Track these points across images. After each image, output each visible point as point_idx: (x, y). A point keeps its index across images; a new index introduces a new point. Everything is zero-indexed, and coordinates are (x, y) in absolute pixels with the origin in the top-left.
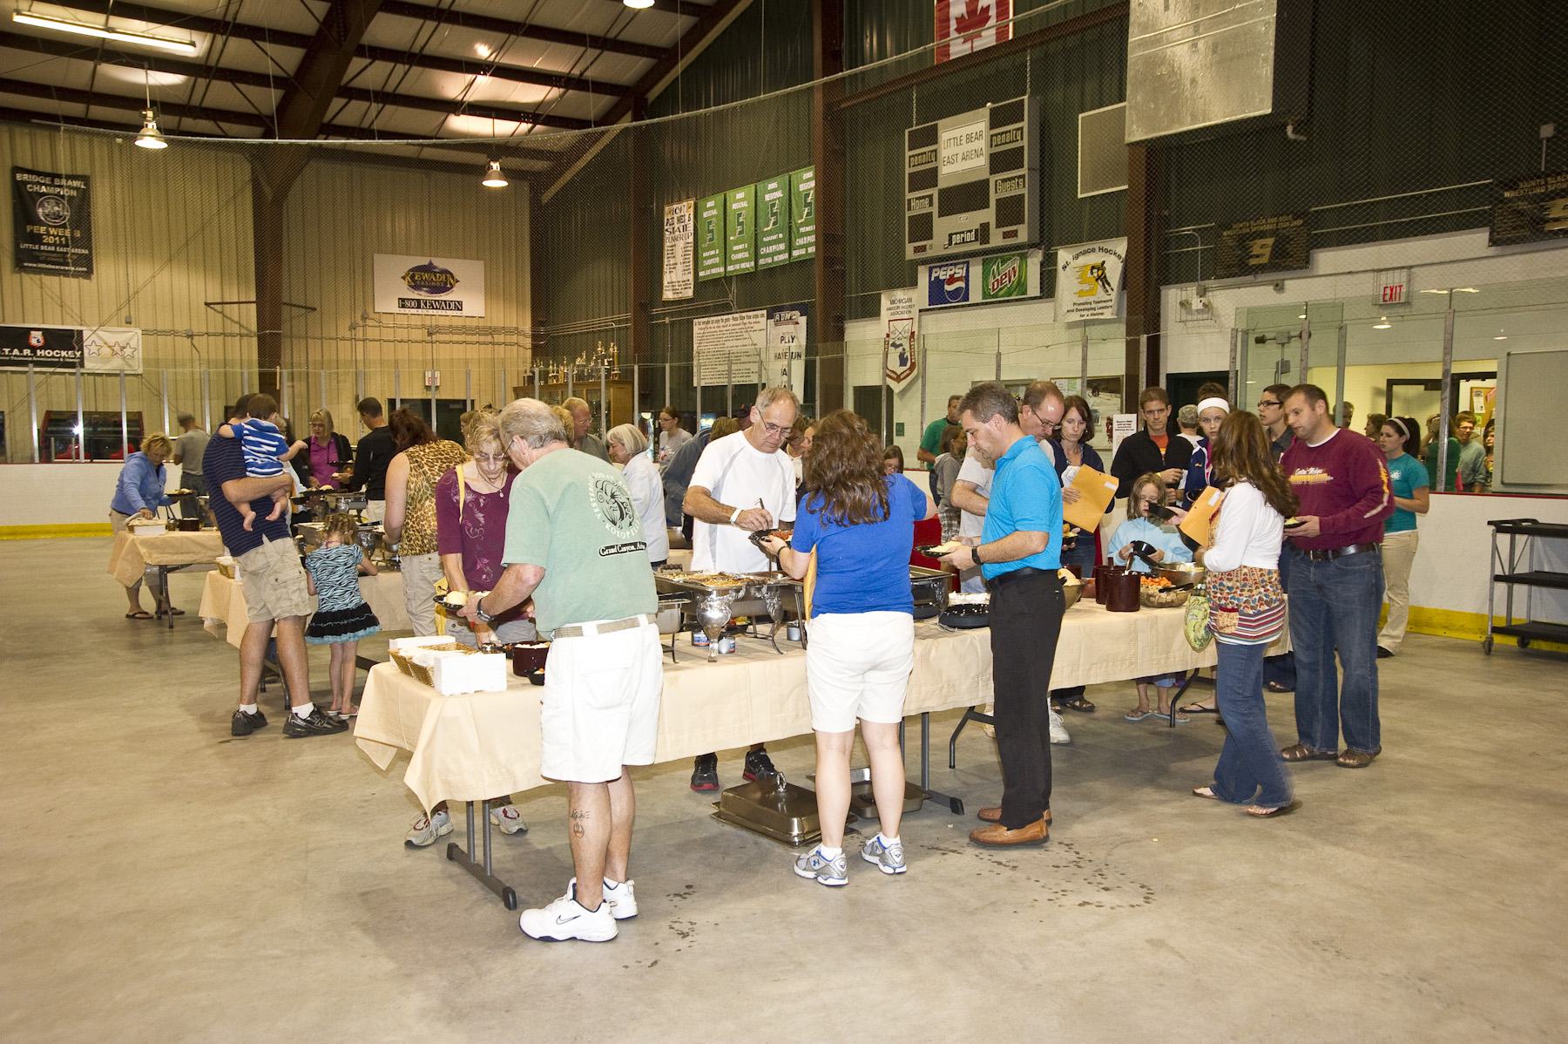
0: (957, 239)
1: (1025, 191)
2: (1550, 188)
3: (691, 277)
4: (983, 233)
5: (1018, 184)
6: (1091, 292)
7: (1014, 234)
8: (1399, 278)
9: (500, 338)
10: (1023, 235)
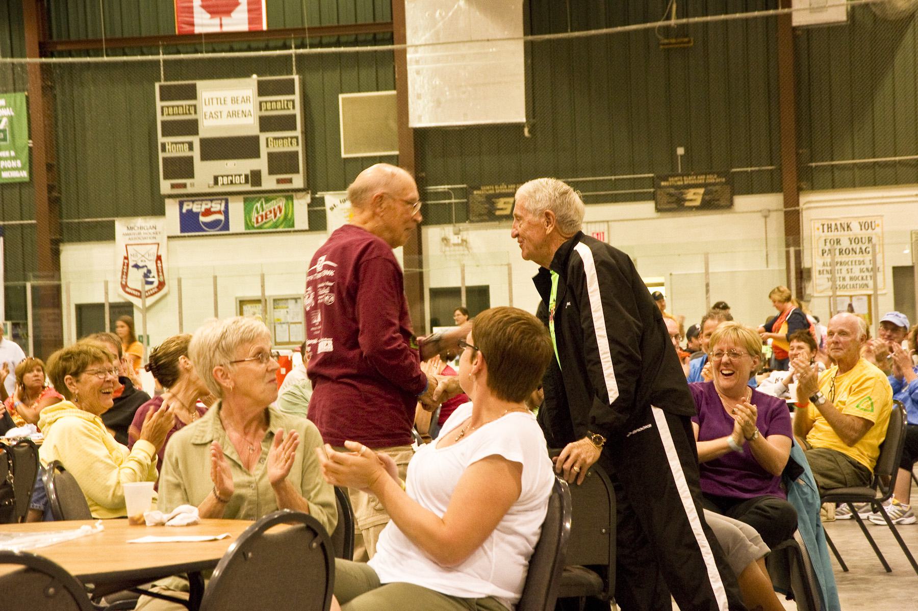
1: (300, 149)
4: (255, 177)
5: (291, 142)
7: (290, 181)
10: (298, 181)
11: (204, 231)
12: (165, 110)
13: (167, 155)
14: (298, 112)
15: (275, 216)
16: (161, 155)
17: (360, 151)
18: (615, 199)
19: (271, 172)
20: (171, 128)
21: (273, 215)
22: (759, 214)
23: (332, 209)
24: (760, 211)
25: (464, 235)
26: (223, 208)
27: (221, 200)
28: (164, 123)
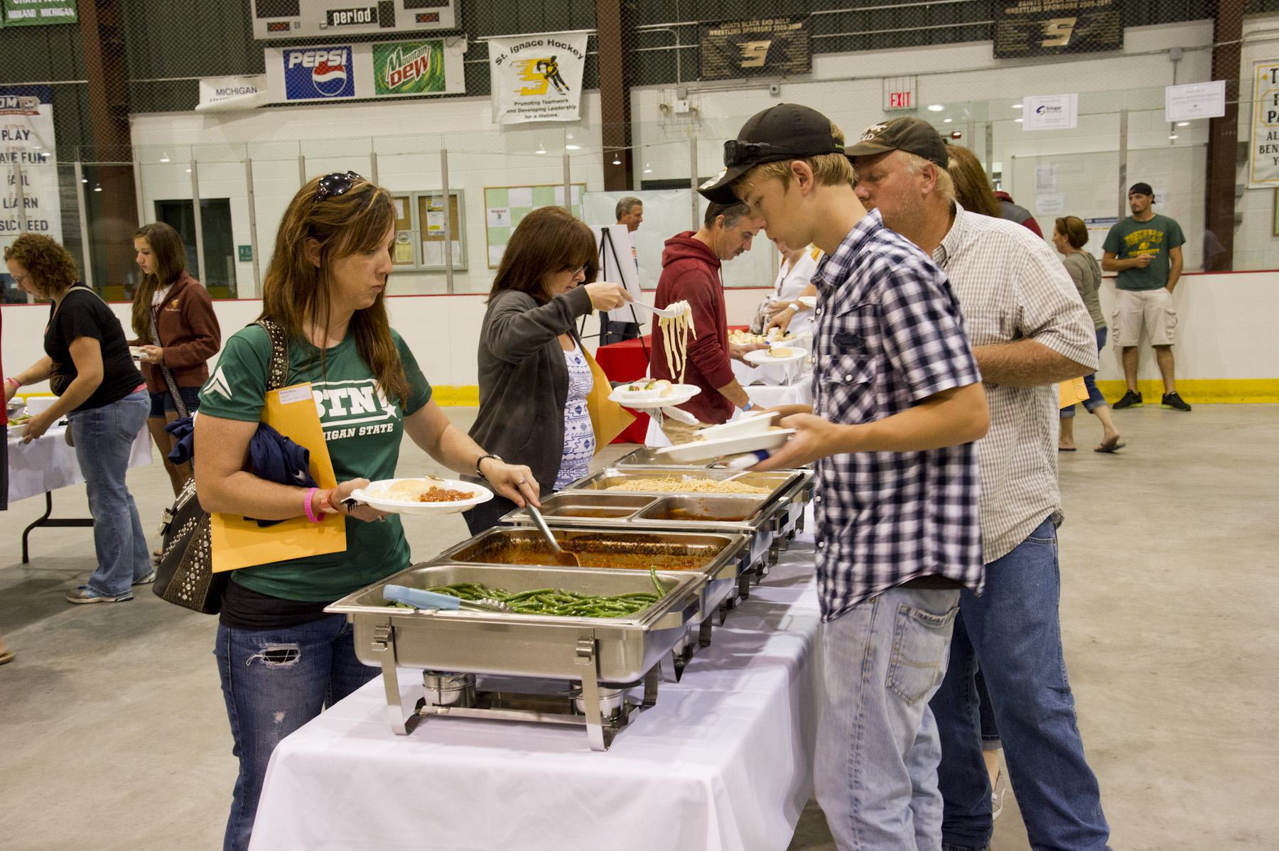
2: (745, 31)
6: (540, 90)
7: (435, 17)
10: (447, 18)
11: (319, 96)
15: (418, 72)
18: (928, 39)
21: (414, 71)
22: (1165, 57)
23: (499, 61)
24: (1168, 51)
25: (695, 100)
26: (344, 63)
27: (343, 49)
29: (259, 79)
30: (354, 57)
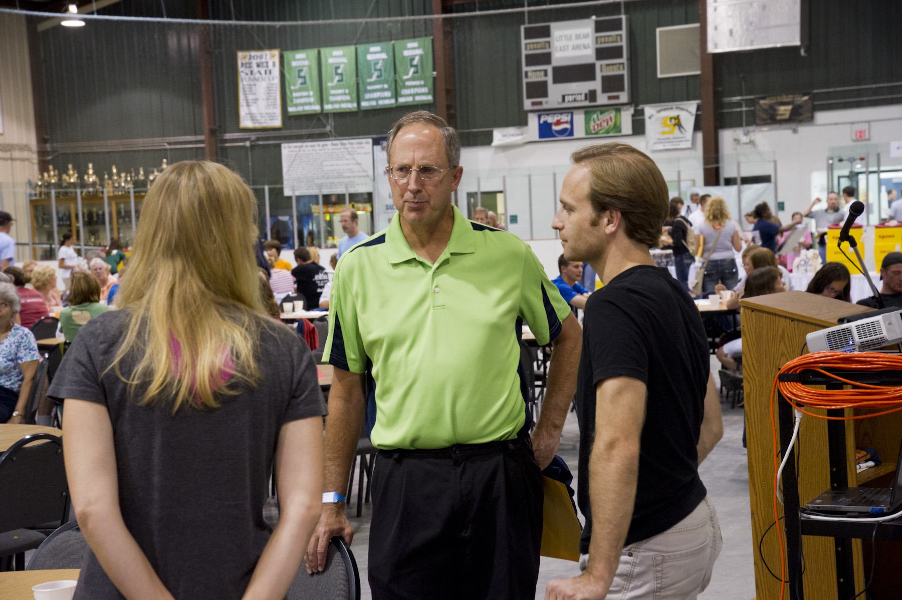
0: (567, 98)
1: (625, 72)
3: (278, 111)
4: (592, 95)
5: (620, 67)
6: (671, 132)
7: (617, 97)
8: (864, 127)
9: (17, 154)
10: (624, 97)
12: (527, 46)
13: (529, 80)
14: (624, 43)
16: (525, 81)
17: (671, 72)
19: (605, 90)
20: (533, 60)
23: (650, 118)
28: (527, 56)
29: (525, 129)
30: (575, 117)
